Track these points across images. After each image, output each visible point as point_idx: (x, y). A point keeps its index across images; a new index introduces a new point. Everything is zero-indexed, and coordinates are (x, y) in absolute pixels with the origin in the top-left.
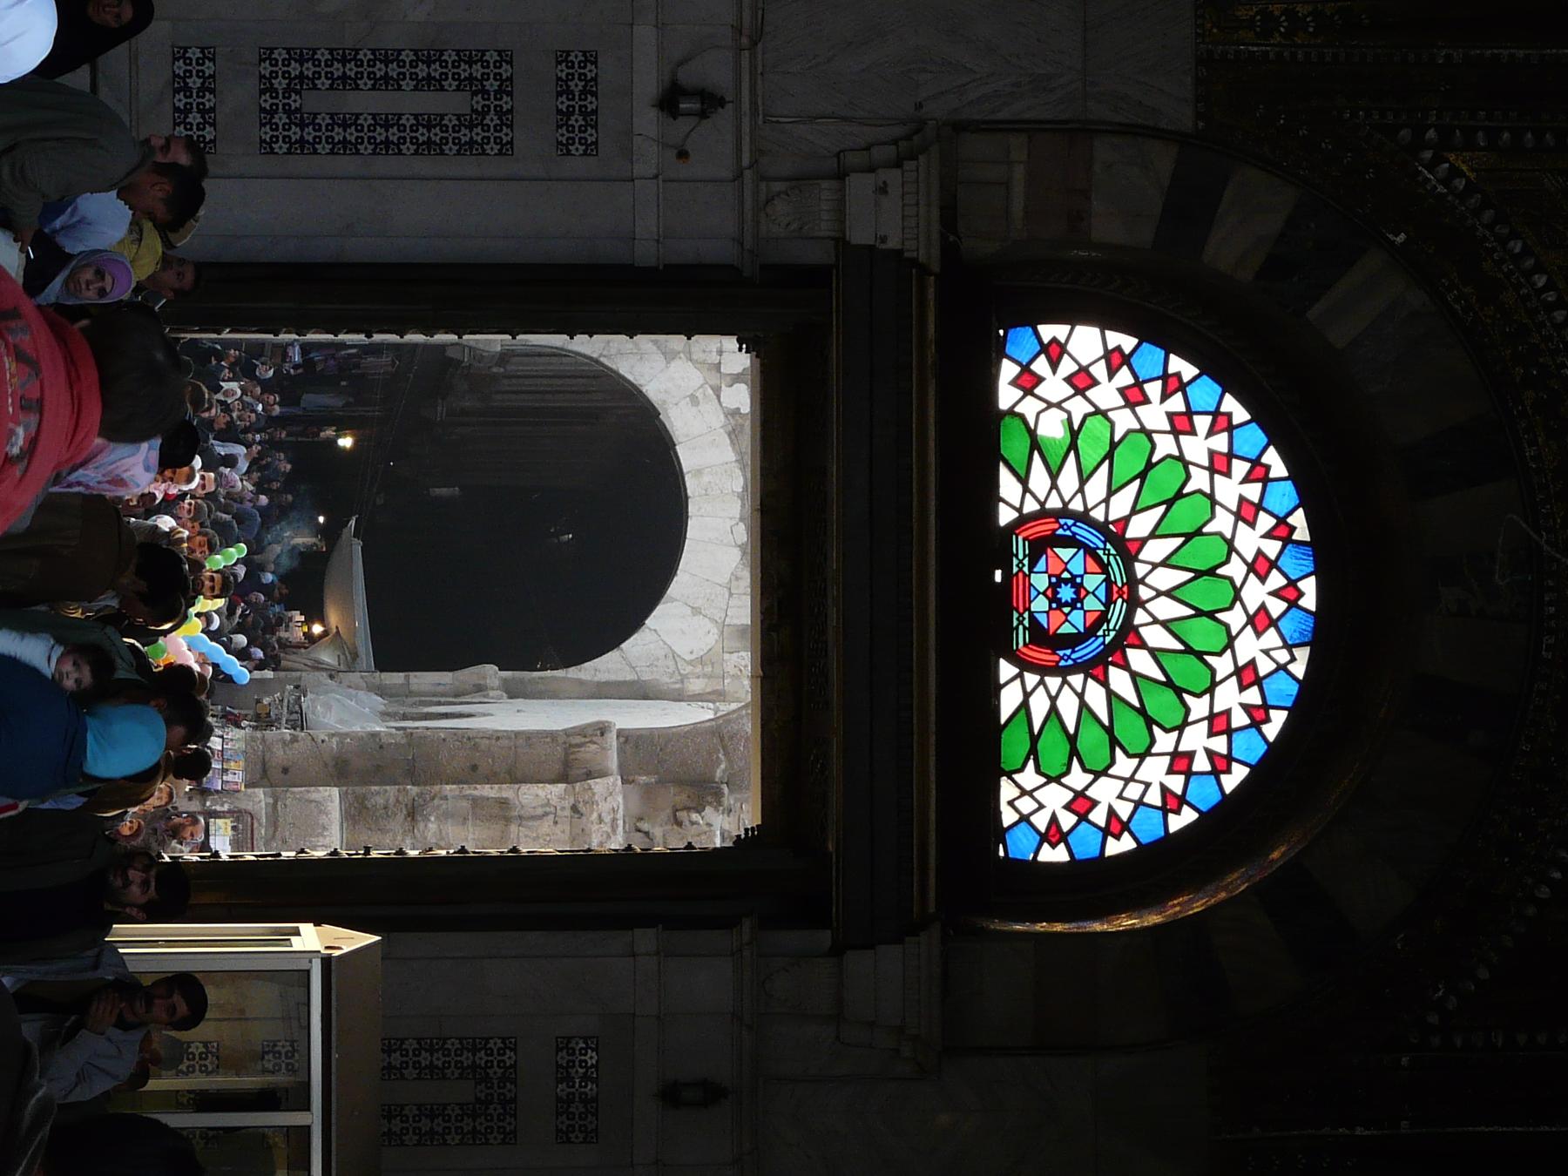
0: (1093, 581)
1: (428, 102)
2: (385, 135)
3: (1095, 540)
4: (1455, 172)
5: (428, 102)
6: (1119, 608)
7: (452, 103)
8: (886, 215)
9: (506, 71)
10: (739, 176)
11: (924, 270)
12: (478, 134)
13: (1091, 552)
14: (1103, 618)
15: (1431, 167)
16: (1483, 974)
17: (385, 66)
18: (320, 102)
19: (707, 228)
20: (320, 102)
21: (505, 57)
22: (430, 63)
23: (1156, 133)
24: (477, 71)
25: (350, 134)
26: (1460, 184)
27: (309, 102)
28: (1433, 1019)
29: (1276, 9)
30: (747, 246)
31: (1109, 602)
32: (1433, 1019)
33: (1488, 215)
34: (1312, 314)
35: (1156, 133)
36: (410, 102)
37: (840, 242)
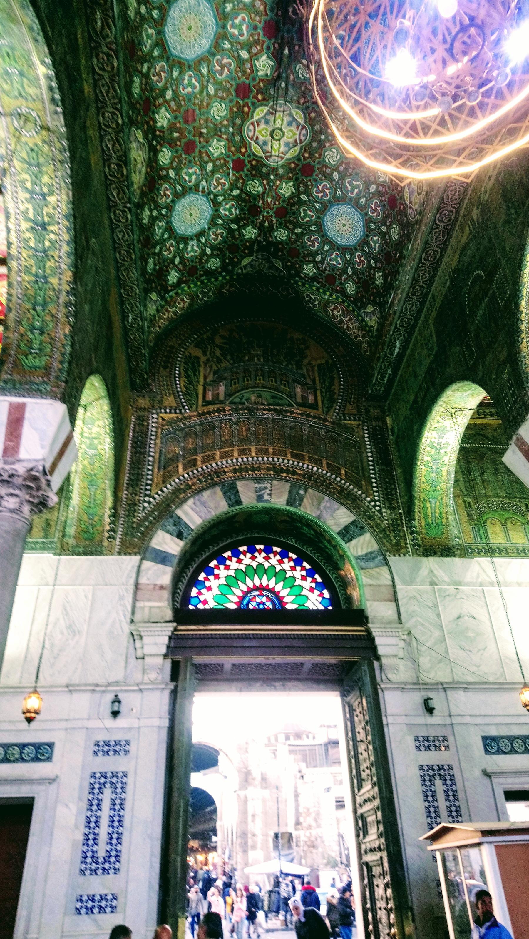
0: (258, 600)
1: (106, 805)
2: (117, 822)
3: (247, 599)
4: (157, 494)
5: (106, 805)
6: (265, 593)
7: (107, 795)
8: (157, 641)
9: (98, 775)
10: (141, 690)
11: (176, 630)
12: (119, 785)
13: (250, 600)
14: (267, 597)
15: (154, 499)
16: (360, 492)
17: (92, 823)
18: (101, 851)
19: (159, 701)
20: (101, 851)
21: (93, 776)
22: (94, 805)
23: (139, 566)
24: (97, 786)
25: (116, 838)
26: (160, 493)
27: (101, 854)
28: (373, 504)
29: (107, 534)
30: (163, 686)
31: (263, 596)
32: (373, 504)
33: (169, 486)
34: (193, 527)
35: (139, 566)
36: (105, 813)
37: (165, 656)
